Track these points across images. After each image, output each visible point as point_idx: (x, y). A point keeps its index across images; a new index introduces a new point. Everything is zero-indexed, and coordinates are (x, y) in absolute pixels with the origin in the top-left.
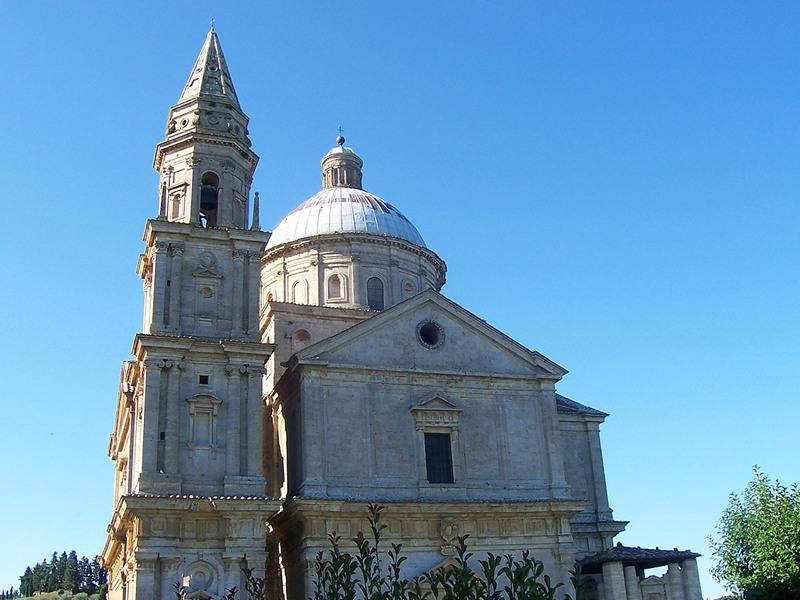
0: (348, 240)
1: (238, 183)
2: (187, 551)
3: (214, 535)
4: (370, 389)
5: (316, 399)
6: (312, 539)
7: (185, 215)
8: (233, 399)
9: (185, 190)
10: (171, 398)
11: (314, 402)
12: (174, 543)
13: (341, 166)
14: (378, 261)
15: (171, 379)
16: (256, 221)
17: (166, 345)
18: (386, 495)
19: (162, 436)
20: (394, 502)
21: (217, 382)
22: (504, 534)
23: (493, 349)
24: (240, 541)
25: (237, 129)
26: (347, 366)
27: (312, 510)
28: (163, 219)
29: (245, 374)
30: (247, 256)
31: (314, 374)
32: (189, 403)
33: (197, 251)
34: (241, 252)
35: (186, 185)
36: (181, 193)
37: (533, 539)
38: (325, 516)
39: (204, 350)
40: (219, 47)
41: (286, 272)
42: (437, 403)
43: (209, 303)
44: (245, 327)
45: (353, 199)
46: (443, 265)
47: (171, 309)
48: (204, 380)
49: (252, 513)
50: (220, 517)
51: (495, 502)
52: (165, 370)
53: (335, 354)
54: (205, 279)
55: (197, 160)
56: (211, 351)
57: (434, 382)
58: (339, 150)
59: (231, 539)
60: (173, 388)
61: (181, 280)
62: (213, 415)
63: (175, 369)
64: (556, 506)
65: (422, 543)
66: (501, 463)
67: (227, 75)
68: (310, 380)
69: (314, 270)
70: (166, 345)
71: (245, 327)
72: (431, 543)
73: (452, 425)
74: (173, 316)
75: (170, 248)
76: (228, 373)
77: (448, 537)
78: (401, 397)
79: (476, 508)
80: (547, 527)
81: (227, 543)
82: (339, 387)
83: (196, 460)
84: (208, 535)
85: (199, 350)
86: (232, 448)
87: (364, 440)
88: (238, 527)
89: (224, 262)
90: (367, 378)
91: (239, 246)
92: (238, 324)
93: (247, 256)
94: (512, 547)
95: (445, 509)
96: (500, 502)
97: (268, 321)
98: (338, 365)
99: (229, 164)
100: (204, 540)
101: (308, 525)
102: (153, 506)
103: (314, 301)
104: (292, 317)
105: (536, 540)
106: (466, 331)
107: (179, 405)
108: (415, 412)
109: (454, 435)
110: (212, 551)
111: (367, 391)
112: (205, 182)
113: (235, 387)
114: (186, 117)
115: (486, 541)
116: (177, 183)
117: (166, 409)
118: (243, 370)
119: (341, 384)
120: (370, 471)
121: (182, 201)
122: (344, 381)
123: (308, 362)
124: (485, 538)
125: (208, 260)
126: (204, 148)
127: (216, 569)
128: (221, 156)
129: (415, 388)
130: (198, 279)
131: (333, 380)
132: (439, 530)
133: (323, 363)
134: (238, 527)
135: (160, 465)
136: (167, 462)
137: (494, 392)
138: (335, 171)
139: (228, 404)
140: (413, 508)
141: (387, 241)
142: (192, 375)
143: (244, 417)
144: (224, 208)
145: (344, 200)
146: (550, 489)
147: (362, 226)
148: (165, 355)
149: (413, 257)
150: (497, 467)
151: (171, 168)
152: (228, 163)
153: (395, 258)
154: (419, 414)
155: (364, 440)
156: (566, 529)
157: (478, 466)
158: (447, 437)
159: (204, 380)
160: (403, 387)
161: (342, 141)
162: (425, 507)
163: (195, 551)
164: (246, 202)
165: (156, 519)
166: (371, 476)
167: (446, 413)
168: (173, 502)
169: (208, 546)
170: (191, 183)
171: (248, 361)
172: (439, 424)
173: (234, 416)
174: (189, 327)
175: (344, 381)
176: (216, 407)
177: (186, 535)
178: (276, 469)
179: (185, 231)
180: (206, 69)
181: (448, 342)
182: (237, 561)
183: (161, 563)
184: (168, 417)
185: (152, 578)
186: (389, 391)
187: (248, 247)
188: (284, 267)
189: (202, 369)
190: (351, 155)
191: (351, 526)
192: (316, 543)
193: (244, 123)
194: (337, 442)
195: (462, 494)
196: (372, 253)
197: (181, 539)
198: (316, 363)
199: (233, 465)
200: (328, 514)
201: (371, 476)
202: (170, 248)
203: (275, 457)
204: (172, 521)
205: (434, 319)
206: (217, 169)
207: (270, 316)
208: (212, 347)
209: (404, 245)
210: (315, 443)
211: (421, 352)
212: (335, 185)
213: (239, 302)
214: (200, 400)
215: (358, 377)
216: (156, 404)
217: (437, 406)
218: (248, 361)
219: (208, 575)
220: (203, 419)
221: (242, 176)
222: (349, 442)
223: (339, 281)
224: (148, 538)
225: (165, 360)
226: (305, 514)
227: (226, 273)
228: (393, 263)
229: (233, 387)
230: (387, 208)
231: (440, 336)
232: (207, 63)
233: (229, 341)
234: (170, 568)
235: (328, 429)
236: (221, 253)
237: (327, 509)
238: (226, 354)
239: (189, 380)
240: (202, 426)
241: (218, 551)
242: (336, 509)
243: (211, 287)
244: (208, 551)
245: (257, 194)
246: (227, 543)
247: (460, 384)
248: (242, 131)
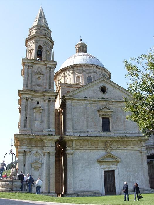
0: (82, 66)
1: (48, 49)
2: (32, 150)
3: (40, 146)
4: (86, 105)
5: (70, 108)
6: (69, 147)
7: (33, 57)
8: (46, 108)
9: (33, 51)
10: (29, 107)
11: (69, 109)
13: (80, 47)
14: (91, 72)
15: (28, 102)
16: (53, 58)
17: (27, 93)
18: (91, 135)
19: (26, 118)
20: (93, 137)
21: (42, 104)
22: (125, 146)
23: (122, 94)
24: (48, 147)
25: (48, 34)
26: (79, 98)
27: (68, 139)
28: (26, 59)
29: (50, 101)
30: (50, 68)
31: (69, 101)
32: (34, 109)
33: (36, 67)
34: (48, 67)
35: (33, 49)
36: (32, 52)
37: (134, 148)
38: (72, 140)
39: (38, 94)
40: (43, 12)
41: (65, 76)
42: (105, 109)
43: (40, 82)
44: (50, 88)
45: (84, 55)
46: (110, 73)
47: (29, 83)
48: (38, 103)
49: (51, 140)
50: (42, 140)
51: (122, 137)
52: (27, 100)
53: (77, 95)
54: (38, 75)
55: (36, 43)
56: (40, 95)
57: (105, 103)
58: (80, 42)
59: (45, 147)
60: (29, 104)
61: (32, 75)
63: (30, 99)
64: (141, 138)
65: (101, 148)
66: (125, 127)
67: (45, 19)
68: (68, 103)
69: (72, 75)
70: (27, 93)
71: (50, 88)
72: (104, 148)
73: (109, 115)
74: (29, 85)
75: (28, 66)
76: (45, 101)
77: (109, 147)
78: (95, 107)
79: (117, 139)
80: (138, 144)
81: (44, 148)
82: (76, 104)
83: (36, 125)
84: (39, 146)
85: (38, 94)
86: (46, 122)
87: (84, 119)
88: (47, 143)
90: (85, 102)
91: (48, 65)
92: (48, 87)
93: (50, 68)
94: (127, 150)
95: (107, 139)
96: (124, 137)
97: (59, 89)
98: (76, 98)
99: (45, 43)
100: (38, 147)
101: (67, 143)
102: (23, 137)
103: (72, 83)
104: (66, 88)
105: (135, 148)
106: (114, 88)
107: (31, 110)
108: (99, 111)
109: (111, 118)
110: (40, 150)
111: (85, 106)
112: (39, 48)
113: (46, 104)
114: (33, 31)
115: (120, 148)
116: (31, 49)
117: (27, 111)
118: (49, 100)
119: (77, 104)
120: (86, 128)
121: (32, 54)
122: (78, 103)
123: (67, 97)
124: (119, 147)
125: (39, 70)
126: (38, 39)
127: (41, 155)
128: (43, 41)
129: (99, 105)
130: (36, 75)
131: (75, 103)
132: (106, 145)
133: (72, 97)
134: (47, 143)
135: (25, 126)
136: (27, 125)
137: (122, 106)
138: (79, 48)
139: (45, 109)
140: (98, 139)
141: (93, 66)
142: (35, 101)
143: (49, 114)
144: (44, 55)
145: (81, 55)
146: (139, 133)
147: (86, 62)
148: (27, 96)
149: (101, 71)
150: (124, 127)
151: (29, 45)
152: (45, 43)
153: (95, 71)
154: (100, 112)
155: (84, 119)
156: (144, 145)
157: (118, 127)
158: (108, 119)
159: (38, 103)
160: (96, 105)
161: (81, 40)
162: (102, 139)
163: (35, 150)
164: (51, 53)
165: (24, 141)
166: (86, 130)
167: (108, 112)
168: (29, 136)
169: (39, 149)
170: (34, 49)
171: (50, 97)
172: (106, 115)
173: (46, 112)
174: (34, 88)
175: (78, 103)
176: (41, 110)
177: (33, 145)
178: (61, 129)
179: (33, 62)
180: (39, 18)
181: (109, 92)
182: (47, 153)
183: (25, 153)
184: (28, 113)
186: (91, 106)
187: (50, 66)
188: (64, 75)
189: (38, 100)
190: (83, 44)
191: (80, 144)
192: (70, 148)
193: (50, 32)
194: (76, 120)
195: (113, 135)
196: (89, 69)
197: (31, 146)
198: (70, 97)
199: (46, 126)
200: (74, 140)
201: (86, 130)
202: (28, 66)
203: (61, 126)
204: (29, 141)
205: (105, 85)
206: (42, 45)
207: (60, 87)
208: (40, 93)
209: (98, 67)
210: (70, 120)
211: (101, 95)
212: (79, 52)
213: (48, 81)
214: (37, 108)
215: (82, 102)
216: (24, 109)
217: (105, 110)
218: (50, 97)
219: (39, 157)
220: (38, 114)
221: (49, 47)
222: (80, 120)
223: (79, 78)
224: (22, 146)
225: (27, 97)
226: (66, 140)
227: (44, 73)
228: (95, 72)
229: (46, 105)
230: (93, 57)
231: (106, 90)
232: (39, 16)
233: (45, 92)
234: (28, 154)
235: (74, 116)
236: (43, 69)
237: (73, 138)
238: (44, 95)
239: (34, 103)
240: (38, 116)
241: (42, 150)
242: (75, 138)
243: (40, 77)
244: (39, 150)
245: (53, 51)
246: (44, 148)
247: (112, 104)
248: (49, 34)
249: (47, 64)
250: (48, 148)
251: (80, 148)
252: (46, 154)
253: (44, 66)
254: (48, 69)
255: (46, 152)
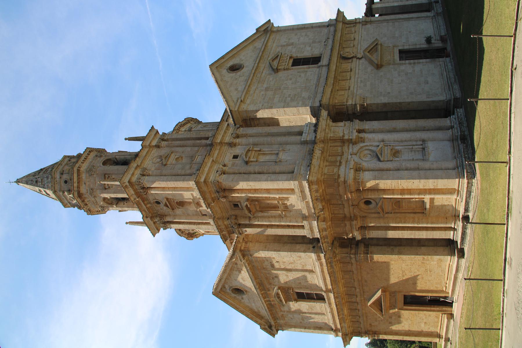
8: (251, 140)
12: (344, 163)
24: (345, 132)
59: (343, 136)
62: (260, 151)
89: (163, 152)
91: (154, 143)
93: (163, 140)
100: (343, 153)
185: (367, 172)
219: (366, 152)
243: (176, 157)
244: (351, 150)
249: (150, 143)
250: (348, 132)
251: (351, 89)
252: (362, 135)
253: (152, 152)
254: (164, 143)
255: (355, 134)
